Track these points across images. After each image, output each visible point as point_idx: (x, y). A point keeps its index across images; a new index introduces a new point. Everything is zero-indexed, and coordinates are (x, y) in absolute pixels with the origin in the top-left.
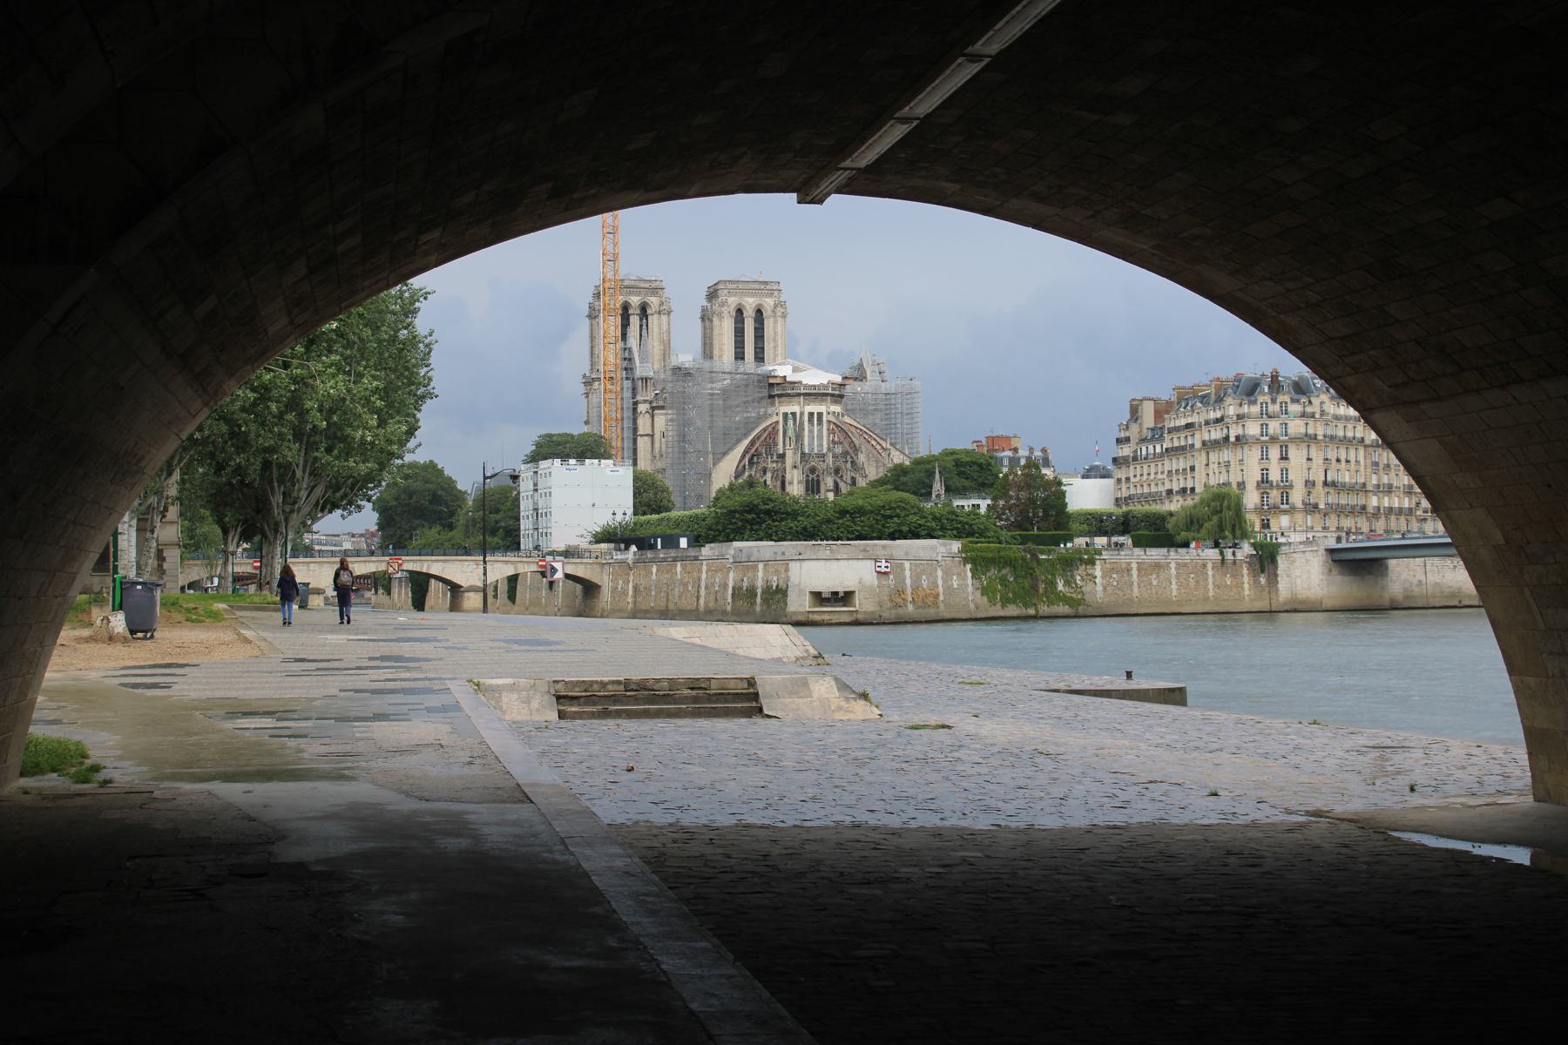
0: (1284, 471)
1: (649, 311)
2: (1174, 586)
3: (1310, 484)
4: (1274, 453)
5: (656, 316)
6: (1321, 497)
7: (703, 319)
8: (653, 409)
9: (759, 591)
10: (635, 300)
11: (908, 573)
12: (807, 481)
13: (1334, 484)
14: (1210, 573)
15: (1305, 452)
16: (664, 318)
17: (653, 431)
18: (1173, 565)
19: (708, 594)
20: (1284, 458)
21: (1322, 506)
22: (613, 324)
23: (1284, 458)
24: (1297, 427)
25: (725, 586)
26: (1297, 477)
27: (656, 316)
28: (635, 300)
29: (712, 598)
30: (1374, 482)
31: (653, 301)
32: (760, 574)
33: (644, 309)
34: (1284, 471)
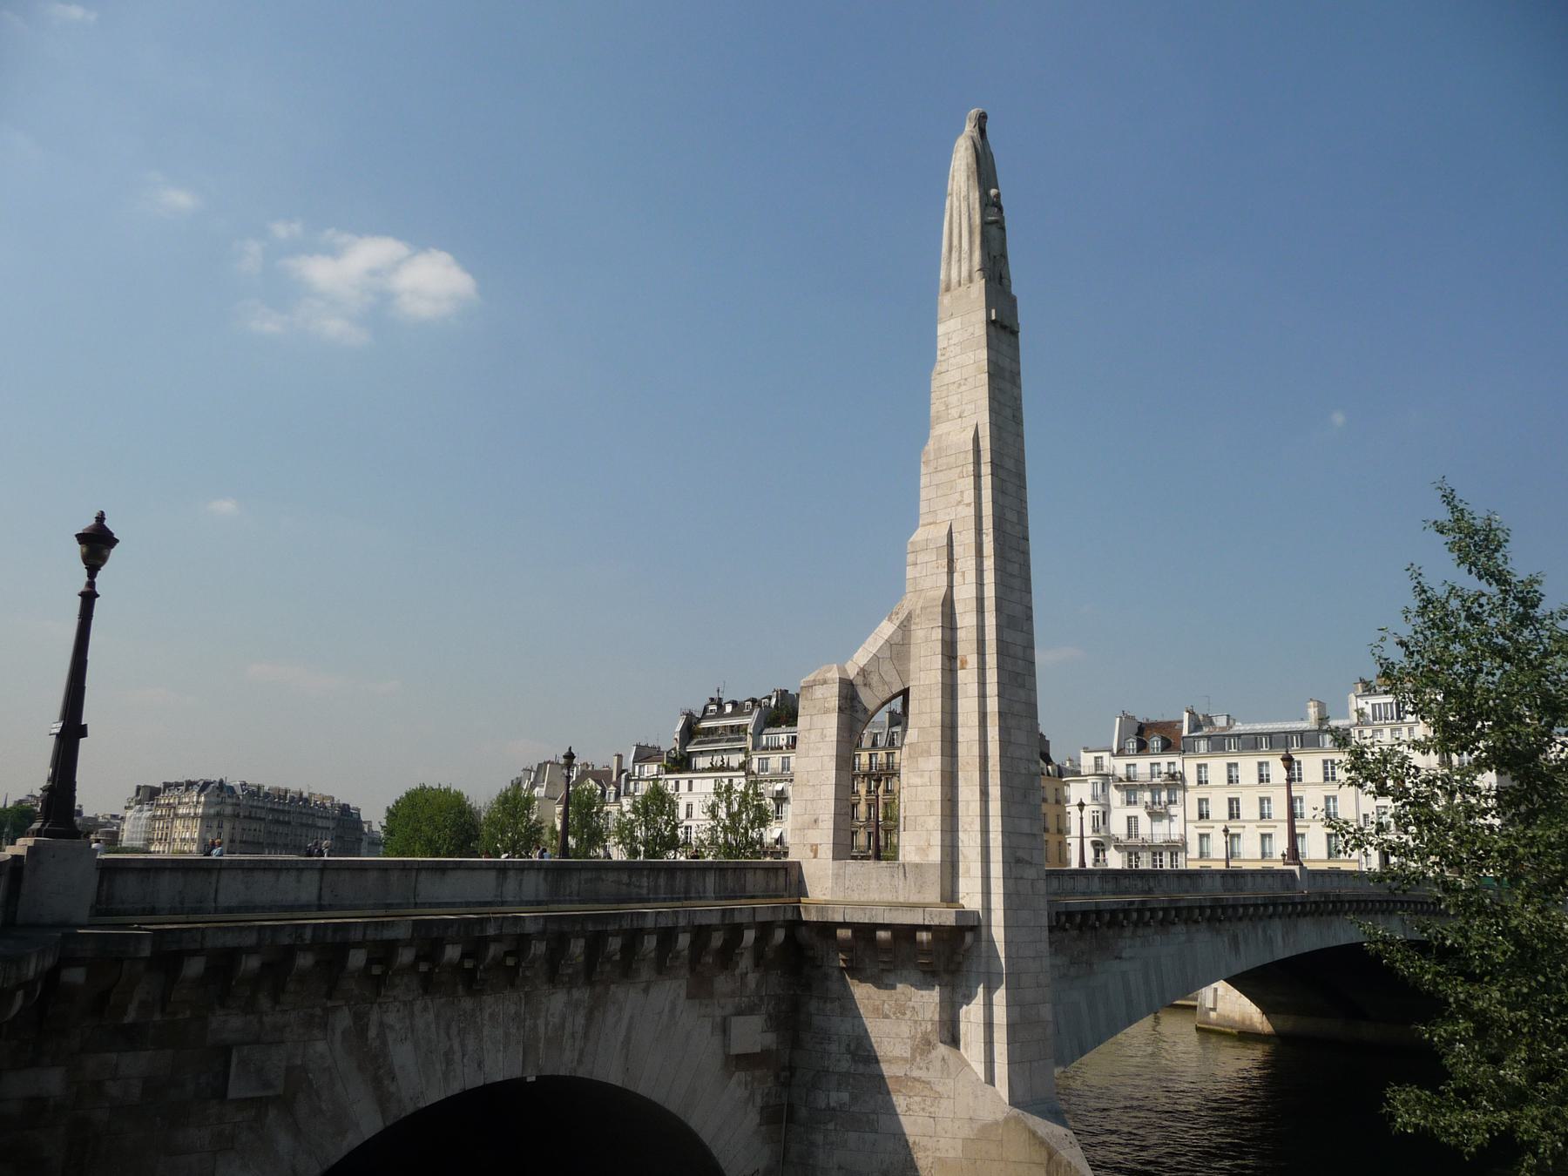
13: (245, 842)
20: (220, 826)
23: (220, 826)
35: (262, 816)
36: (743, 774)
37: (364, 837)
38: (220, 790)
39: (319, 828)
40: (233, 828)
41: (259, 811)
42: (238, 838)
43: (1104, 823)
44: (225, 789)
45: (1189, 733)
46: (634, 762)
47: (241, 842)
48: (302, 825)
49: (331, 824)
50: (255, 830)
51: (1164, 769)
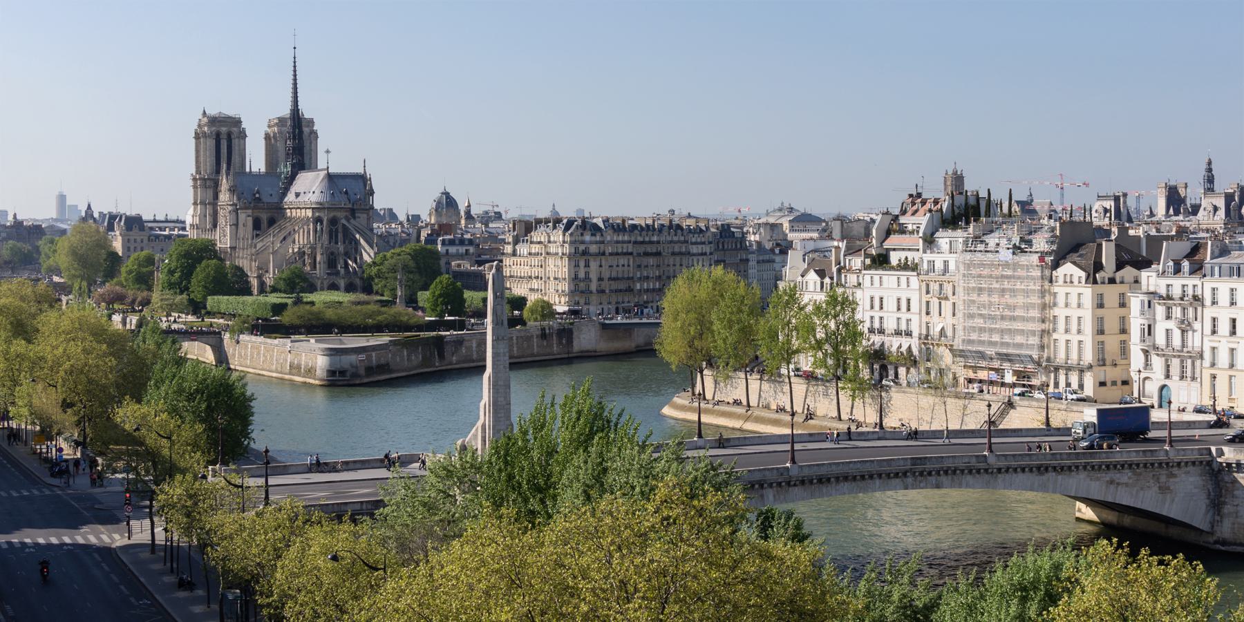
0: (587, 273)
1: (233, 137)
2: (515, 349)
3: (600, 279)
4: (582, 264)
5: (237, 140)
6: (606, 285)
7: (266, 139)
8: (237, 210)
9: (303, 367)
10: (224, 130)
11: (374, 358)
12: (329, 260)
14: (535, 340)
15: (598, 263)
16: (242, 141)
17: (238, 222)
18: (514, 338)
19: (277, 363)
20: (587, 265)
21: (607, 291)
22: (211, 143)
23: (587, 265)
24: (593, 249)
25: (286, 360)
26: (594, 276)
27: (237, 140)
28: (224, 130)
29: (279, 366)
30: (639, 276)
31: (235, 129)
32: (303, 358)
33: (229, 135)
34: (587, 273)
35: (630, 251)
36: (915, 273)
37: (750, 256)
38: (582, 227)
39: (694, 255)
40: (601, 266)
41: (625, 245)
42: (606, 275)
43: (1149, 334)
44: (588, 226)
45: (1211, 259)
46: (845, 256)
47: (610, 279)
48: (673, 254)
49: (707, 249)
50: (623, 266)
51: (1190, 292)
